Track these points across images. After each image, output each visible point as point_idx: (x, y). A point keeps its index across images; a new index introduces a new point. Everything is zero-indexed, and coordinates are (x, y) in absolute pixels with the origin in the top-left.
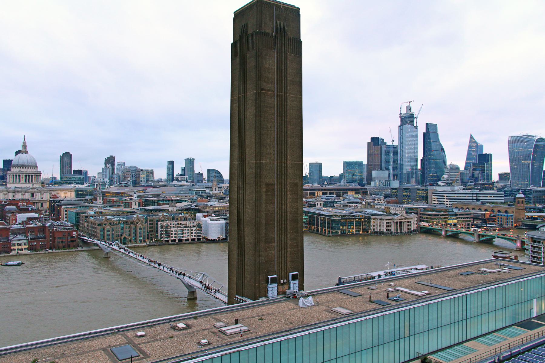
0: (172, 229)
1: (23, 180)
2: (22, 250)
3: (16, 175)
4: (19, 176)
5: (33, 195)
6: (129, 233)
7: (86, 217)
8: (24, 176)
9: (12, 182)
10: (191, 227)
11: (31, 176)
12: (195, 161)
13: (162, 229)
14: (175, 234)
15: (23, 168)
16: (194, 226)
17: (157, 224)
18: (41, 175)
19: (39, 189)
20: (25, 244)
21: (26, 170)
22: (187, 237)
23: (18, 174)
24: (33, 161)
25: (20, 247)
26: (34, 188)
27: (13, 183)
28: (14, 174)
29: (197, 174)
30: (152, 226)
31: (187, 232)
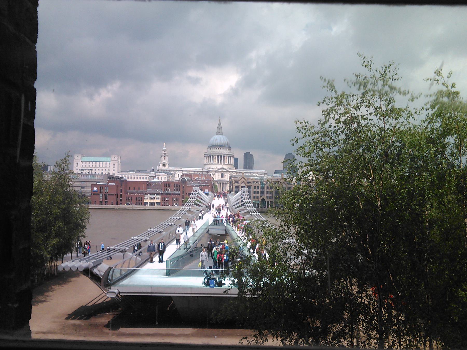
3: (210, 156)
4: (213, 156)
6: (270, 195)
11: (222, 157)
15: (216, 149)
19: (228, 169)
21: (218, 151)
24: (227, 143)
25: (152, 201)
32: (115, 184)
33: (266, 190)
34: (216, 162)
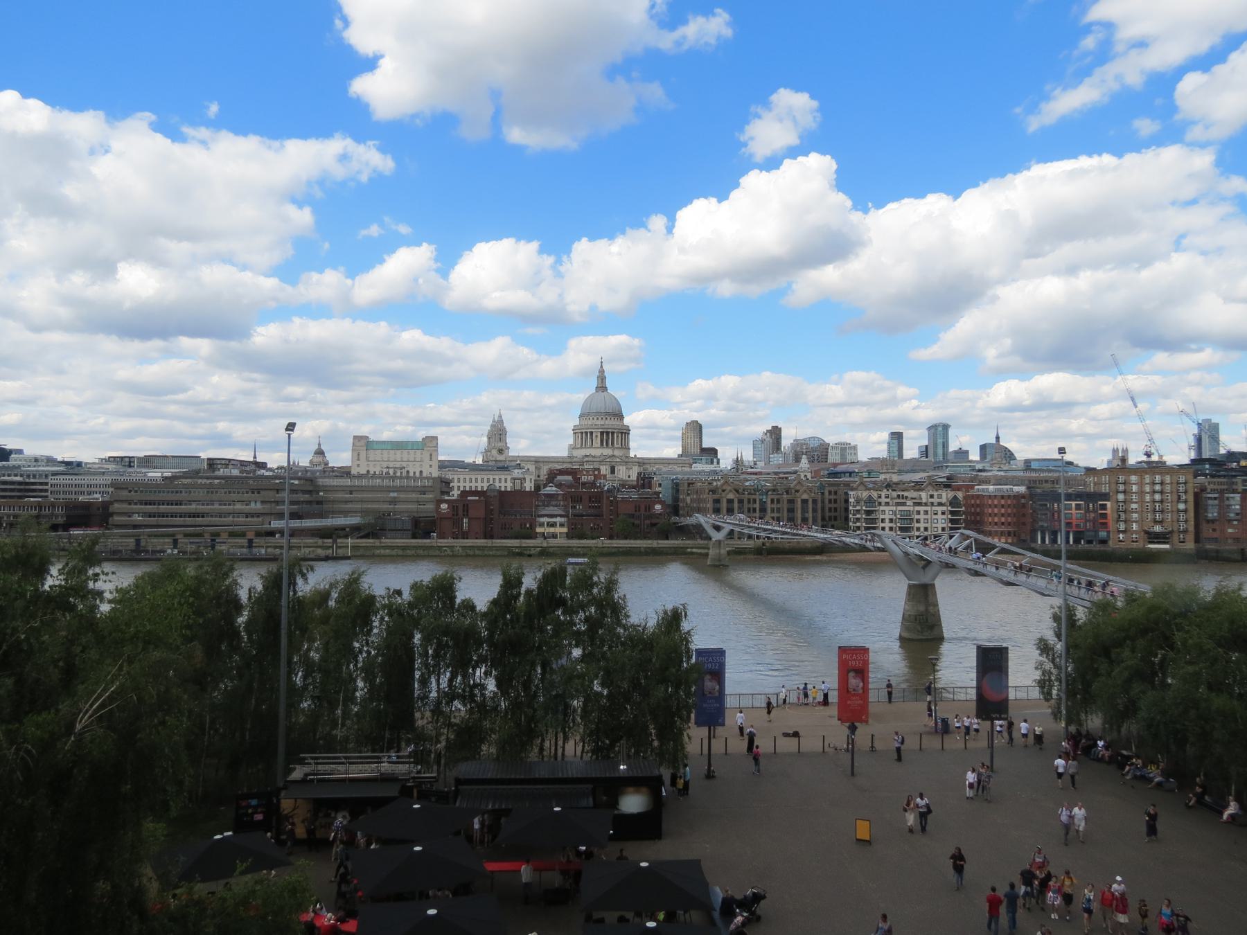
0: (882, 508)
1: (597, 442)
2: (556, 537)
4: (591, 433)
5: (613, 471)
7: (689, 484)
8: (599, 434)
9: (579, 446)
10: (932, 504)
12: (951, 432)
13: (858, 508)
14: (891, 520)
16: (940, 504)
17: (847, 501)
18: (629, 434)
20: (562, 525)
21: (602, 422)
22: (922, 529)
23: (589, 431)
25: (552, 530)
26: (613, 456)
27: (581, 447)
28: (584, 431)
29: (956, 452)
30: (835, 497)
31: (922, 517)
32: (477, 498)
33: (769, 506)
34: (599, 445)
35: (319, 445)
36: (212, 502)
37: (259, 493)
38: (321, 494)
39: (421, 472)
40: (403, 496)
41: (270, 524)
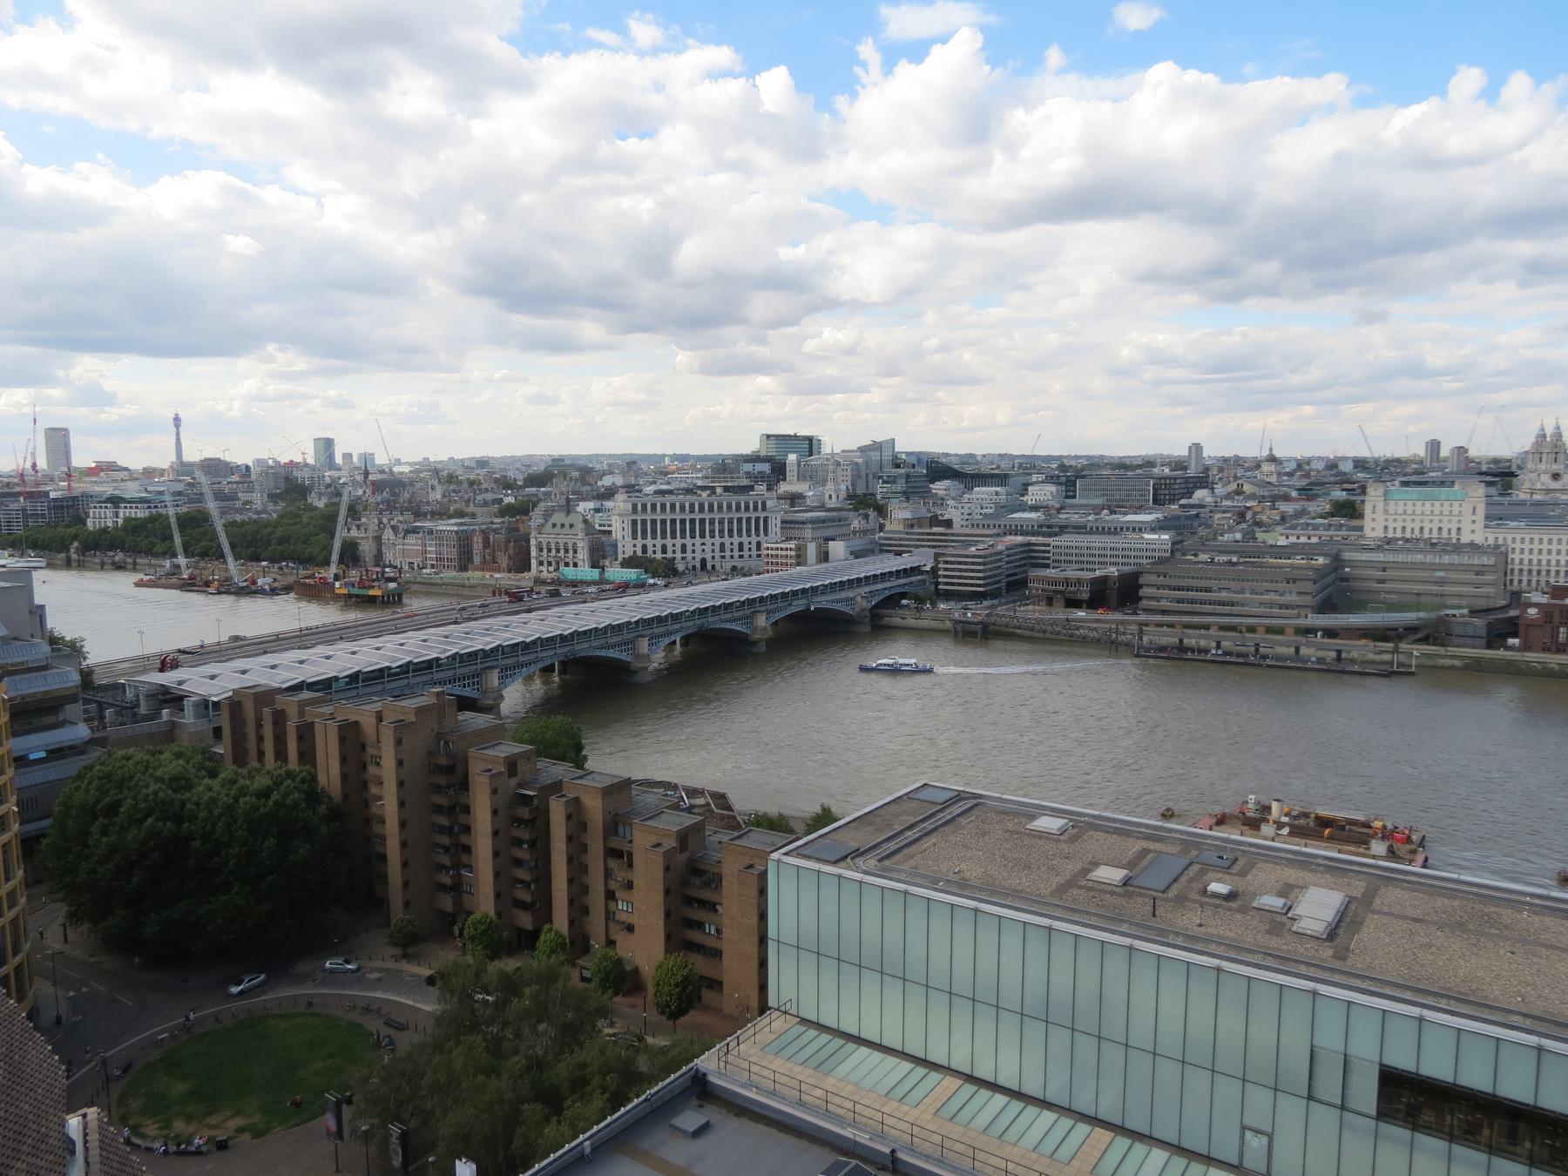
35: (1271, 449)
36: (1242, 591)
37: (1294, 582)
38: (1347, 570)
39: (1459, 529)
40: (1453, 576)
41: (1306, 616)
